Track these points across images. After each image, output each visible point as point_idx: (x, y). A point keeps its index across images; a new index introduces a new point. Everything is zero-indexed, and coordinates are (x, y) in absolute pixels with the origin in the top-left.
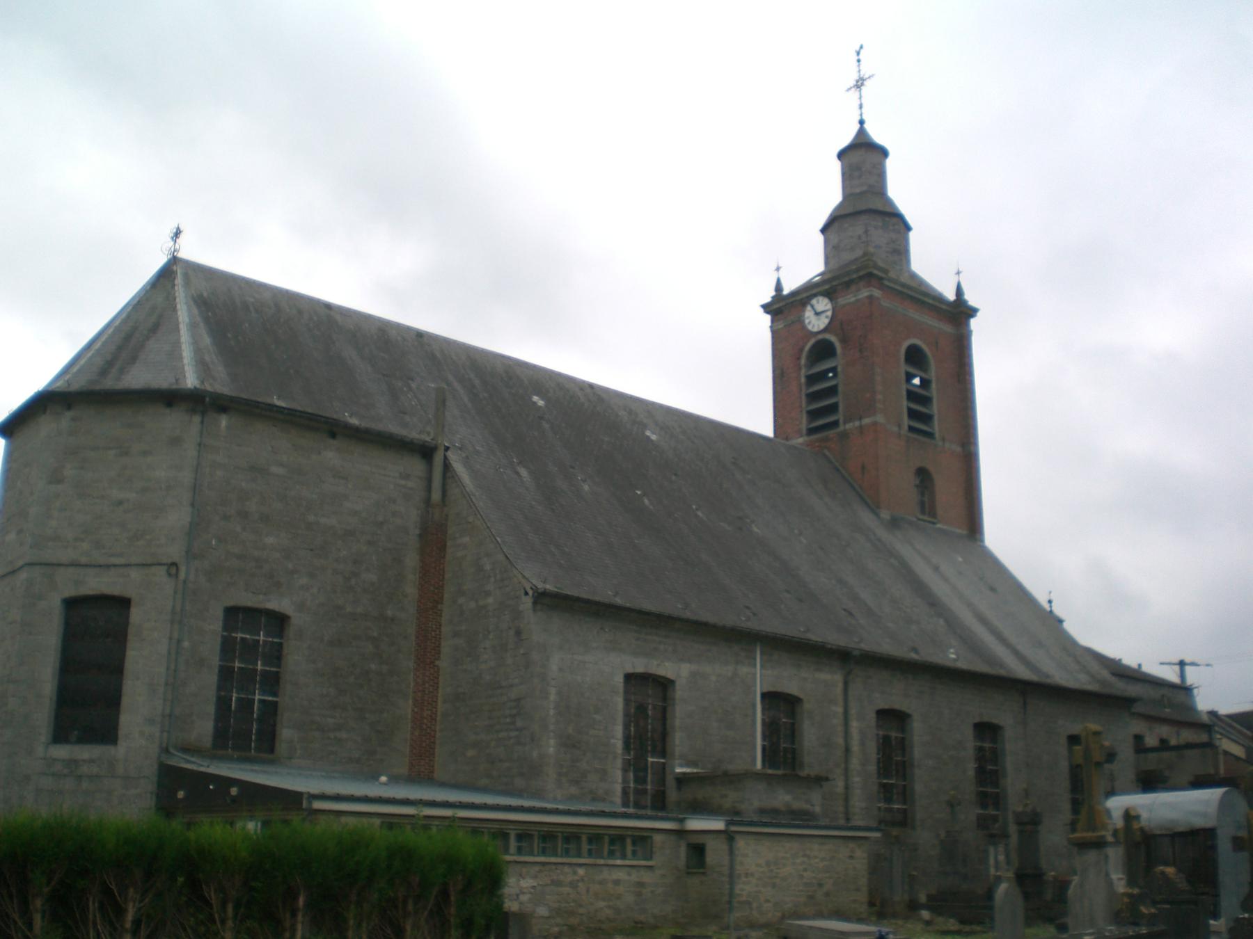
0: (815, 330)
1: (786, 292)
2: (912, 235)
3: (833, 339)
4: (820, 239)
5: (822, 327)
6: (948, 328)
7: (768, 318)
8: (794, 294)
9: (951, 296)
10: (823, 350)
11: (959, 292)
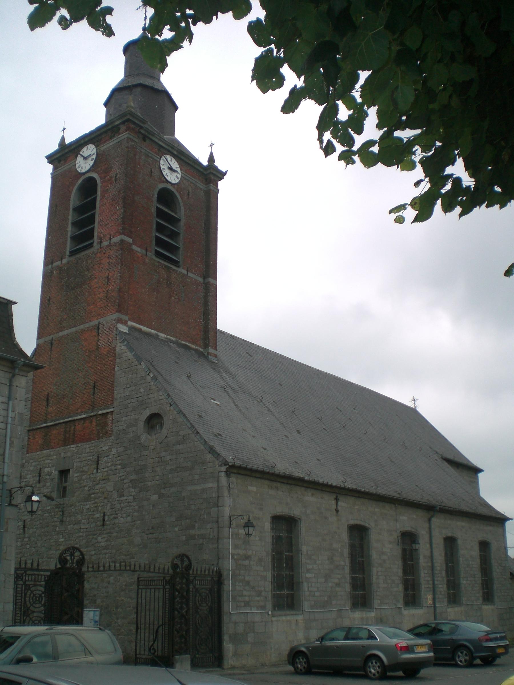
0: (83, 171)
1: (67, 142)
2: (177, 114)
3: (95, 175)
4: (104, 109)
5: (88, 167)
6: (201, 185)
7: (50, 167)
8: (71, 144)
9: (205, 162)
10: (89, 187)
11: (211, 159)
